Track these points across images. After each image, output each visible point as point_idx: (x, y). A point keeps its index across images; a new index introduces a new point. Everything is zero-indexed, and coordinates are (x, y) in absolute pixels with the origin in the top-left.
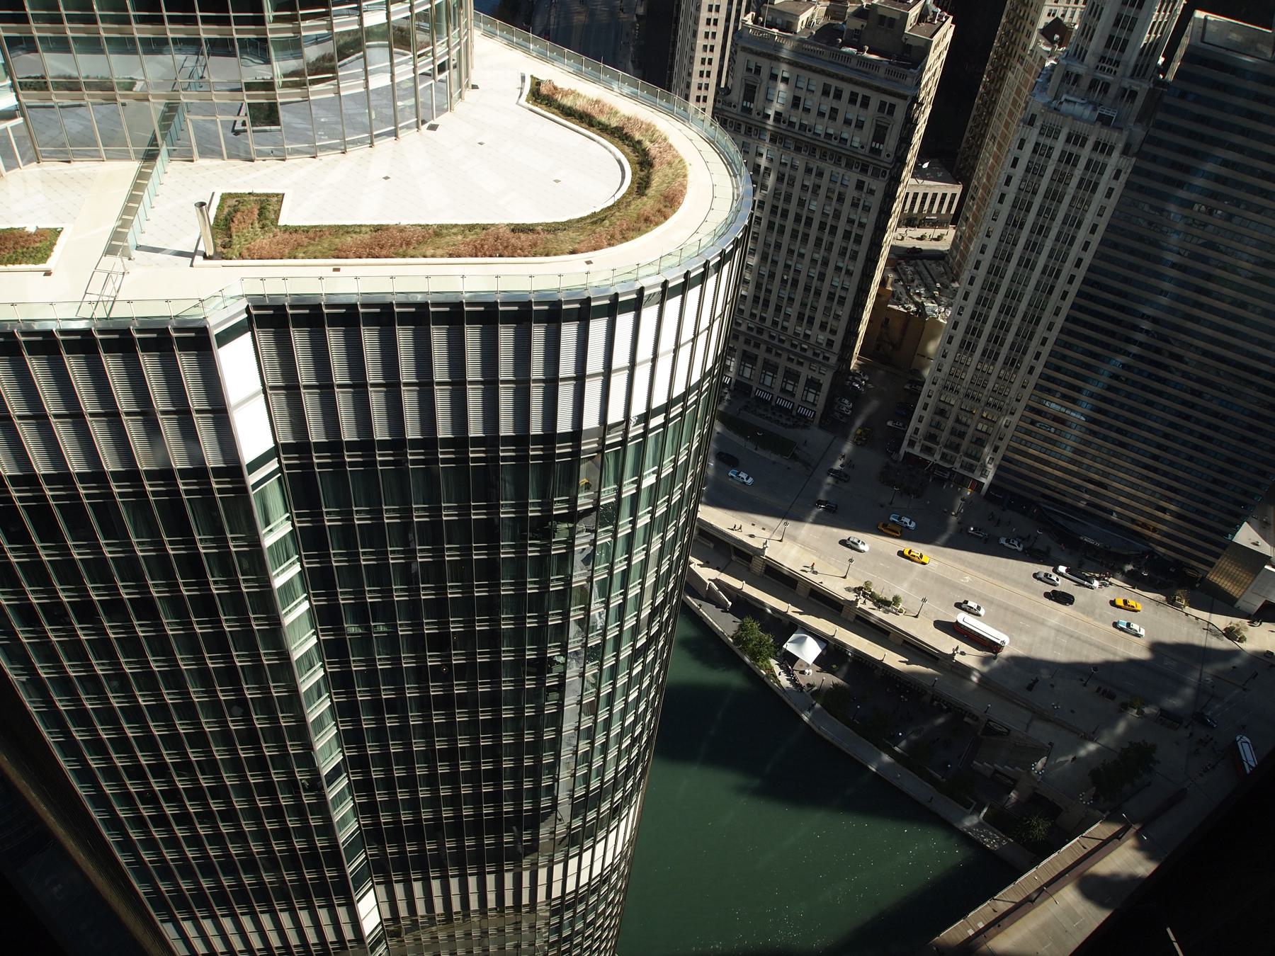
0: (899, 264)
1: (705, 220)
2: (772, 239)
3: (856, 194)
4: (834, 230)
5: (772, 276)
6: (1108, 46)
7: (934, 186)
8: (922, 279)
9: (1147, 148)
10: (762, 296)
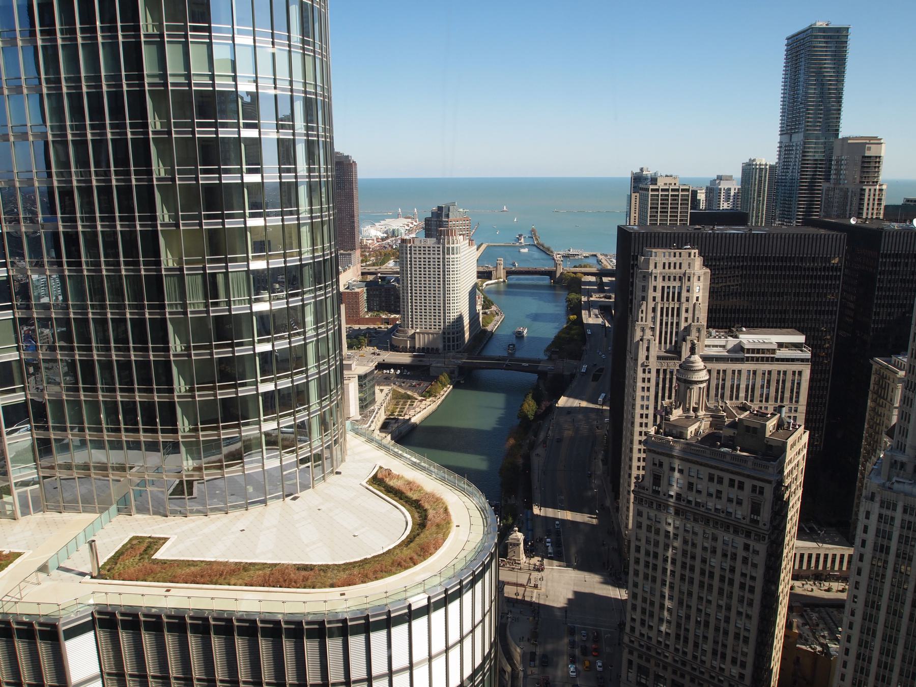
0: (806, 611)
2: (685, 588)
3: (745, 554)
4: (731, 582)
5: (688, 617)
7: (832, 549)
8: (825, 624)
10: (682, 633)
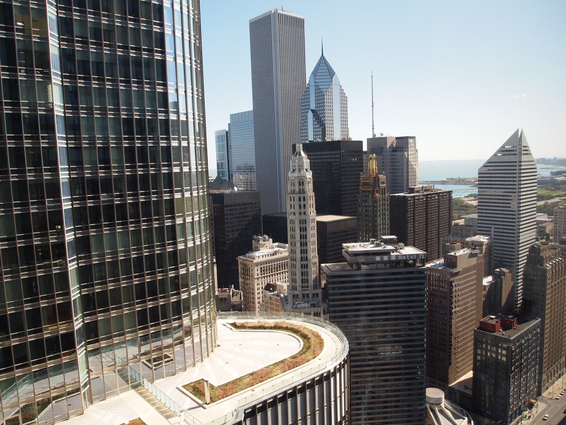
1: (332, 339)
6: (302, 282)
9: (330, 309)
